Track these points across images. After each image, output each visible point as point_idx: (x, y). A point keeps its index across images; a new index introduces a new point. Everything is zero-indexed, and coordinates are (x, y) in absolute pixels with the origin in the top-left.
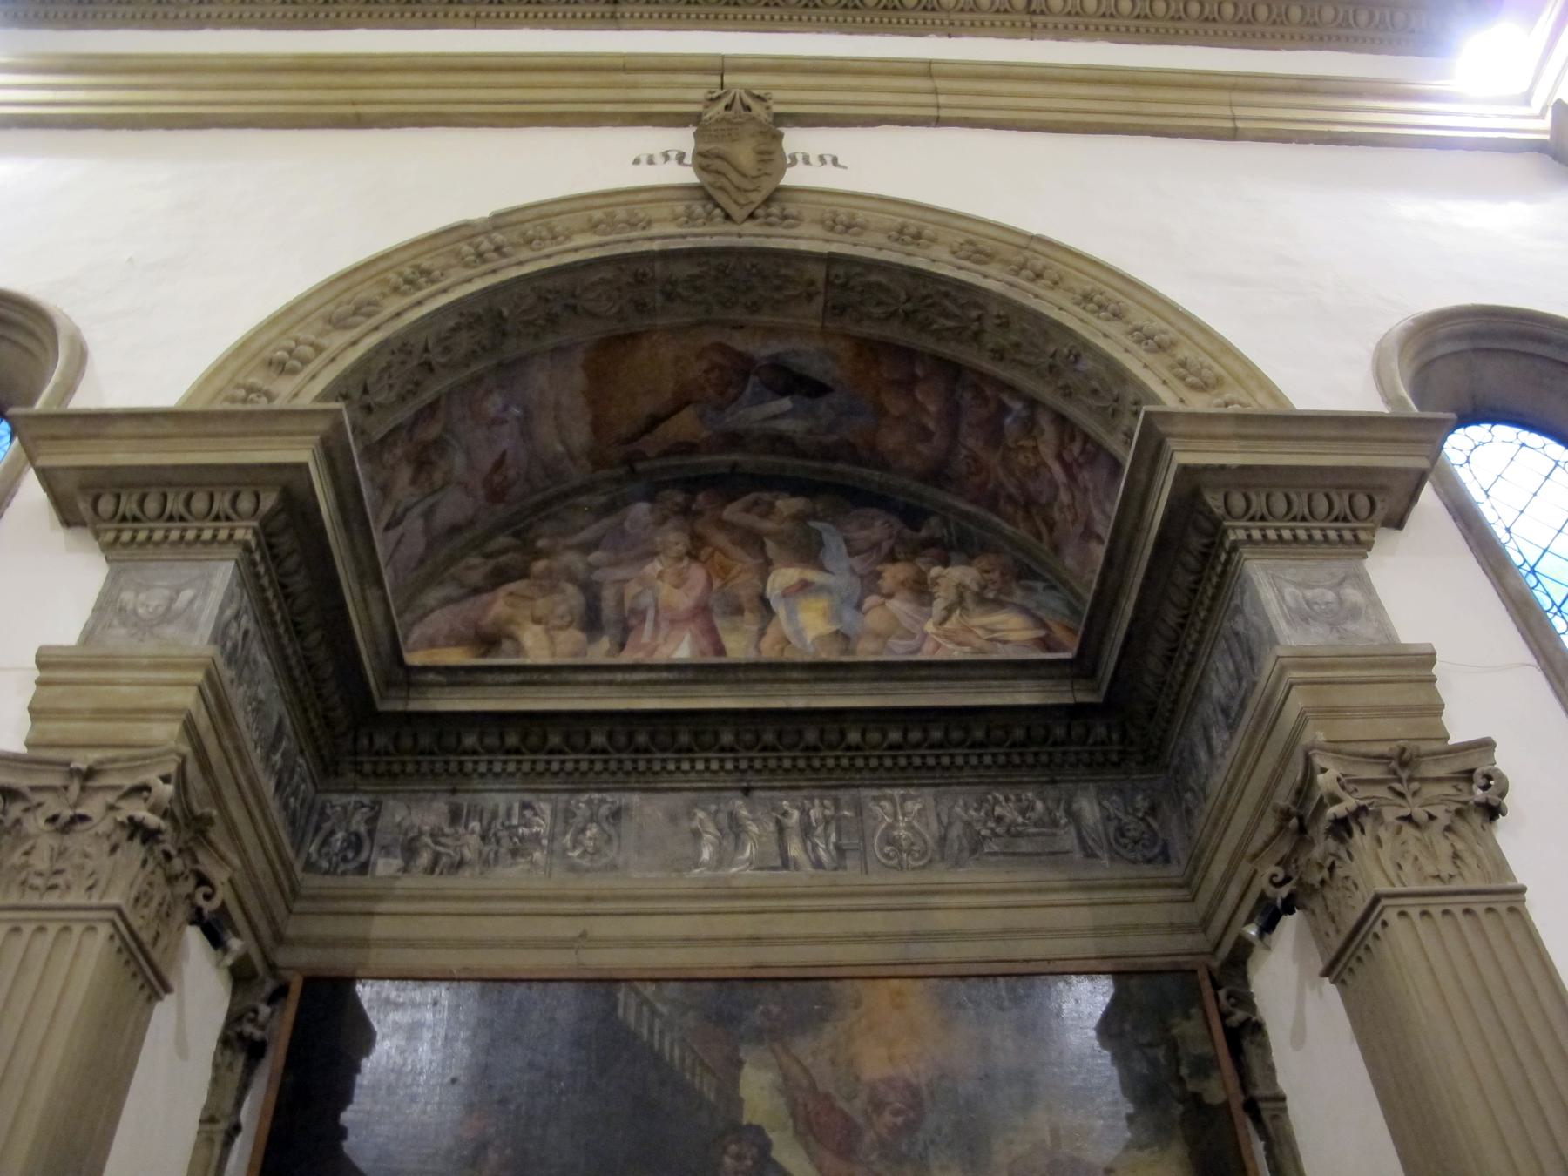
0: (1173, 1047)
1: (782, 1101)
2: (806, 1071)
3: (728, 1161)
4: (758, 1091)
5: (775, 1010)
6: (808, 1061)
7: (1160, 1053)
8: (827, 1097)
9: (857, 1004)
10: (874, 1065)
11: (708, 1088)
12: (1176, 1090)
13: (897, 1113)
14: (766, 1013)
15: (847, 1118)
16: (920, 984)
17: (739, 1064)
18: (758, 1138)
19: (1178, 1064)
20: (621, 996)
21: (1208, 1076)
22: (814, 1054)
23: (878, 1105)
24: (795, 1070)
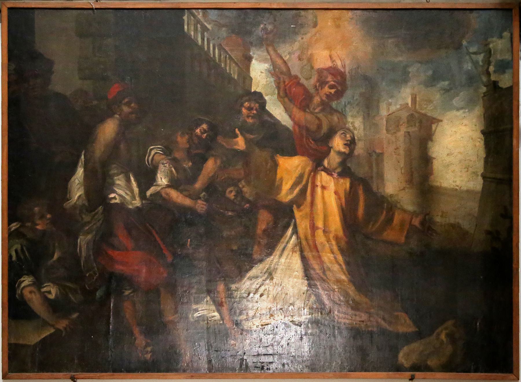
0: (489, 53)
1: (272, 79)
2: (285, 62)
3: (244, 111)
4: (260, 74)
5: (270, 27)
6: (286, 59)
7: (480, 58)
8: (296, 77)
9: (315, 25)
10: (322, 59)
11: (234, 72)
12: (484, 79)
13: (331, 87)
14: (265, 29)
15: (306, 90)
16: (350, 14)
17: (249, 59)
18: (259, 97)
19: (489, 64)
20: (185, 18)
21: (504, 72)
22: (289, 53)
23: (322, 83)
24: (279, 62)
